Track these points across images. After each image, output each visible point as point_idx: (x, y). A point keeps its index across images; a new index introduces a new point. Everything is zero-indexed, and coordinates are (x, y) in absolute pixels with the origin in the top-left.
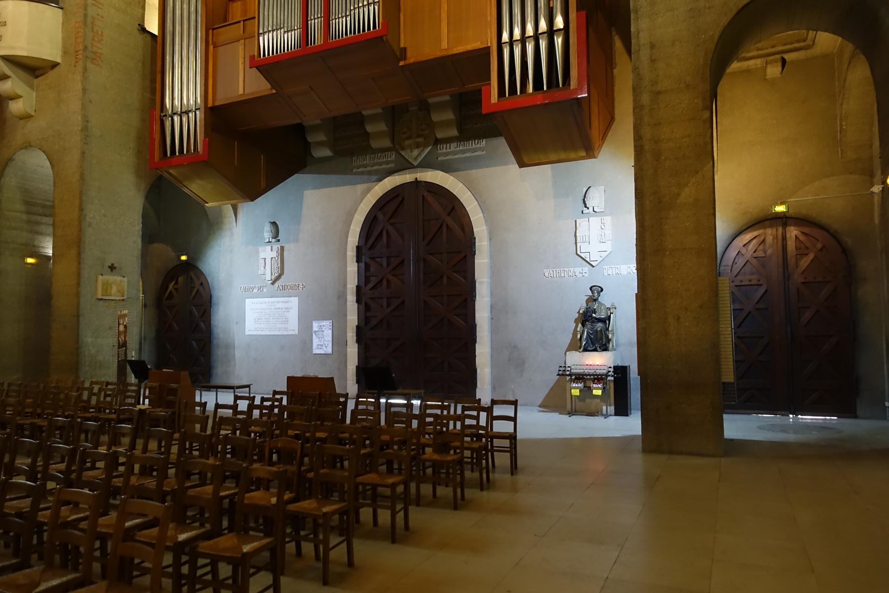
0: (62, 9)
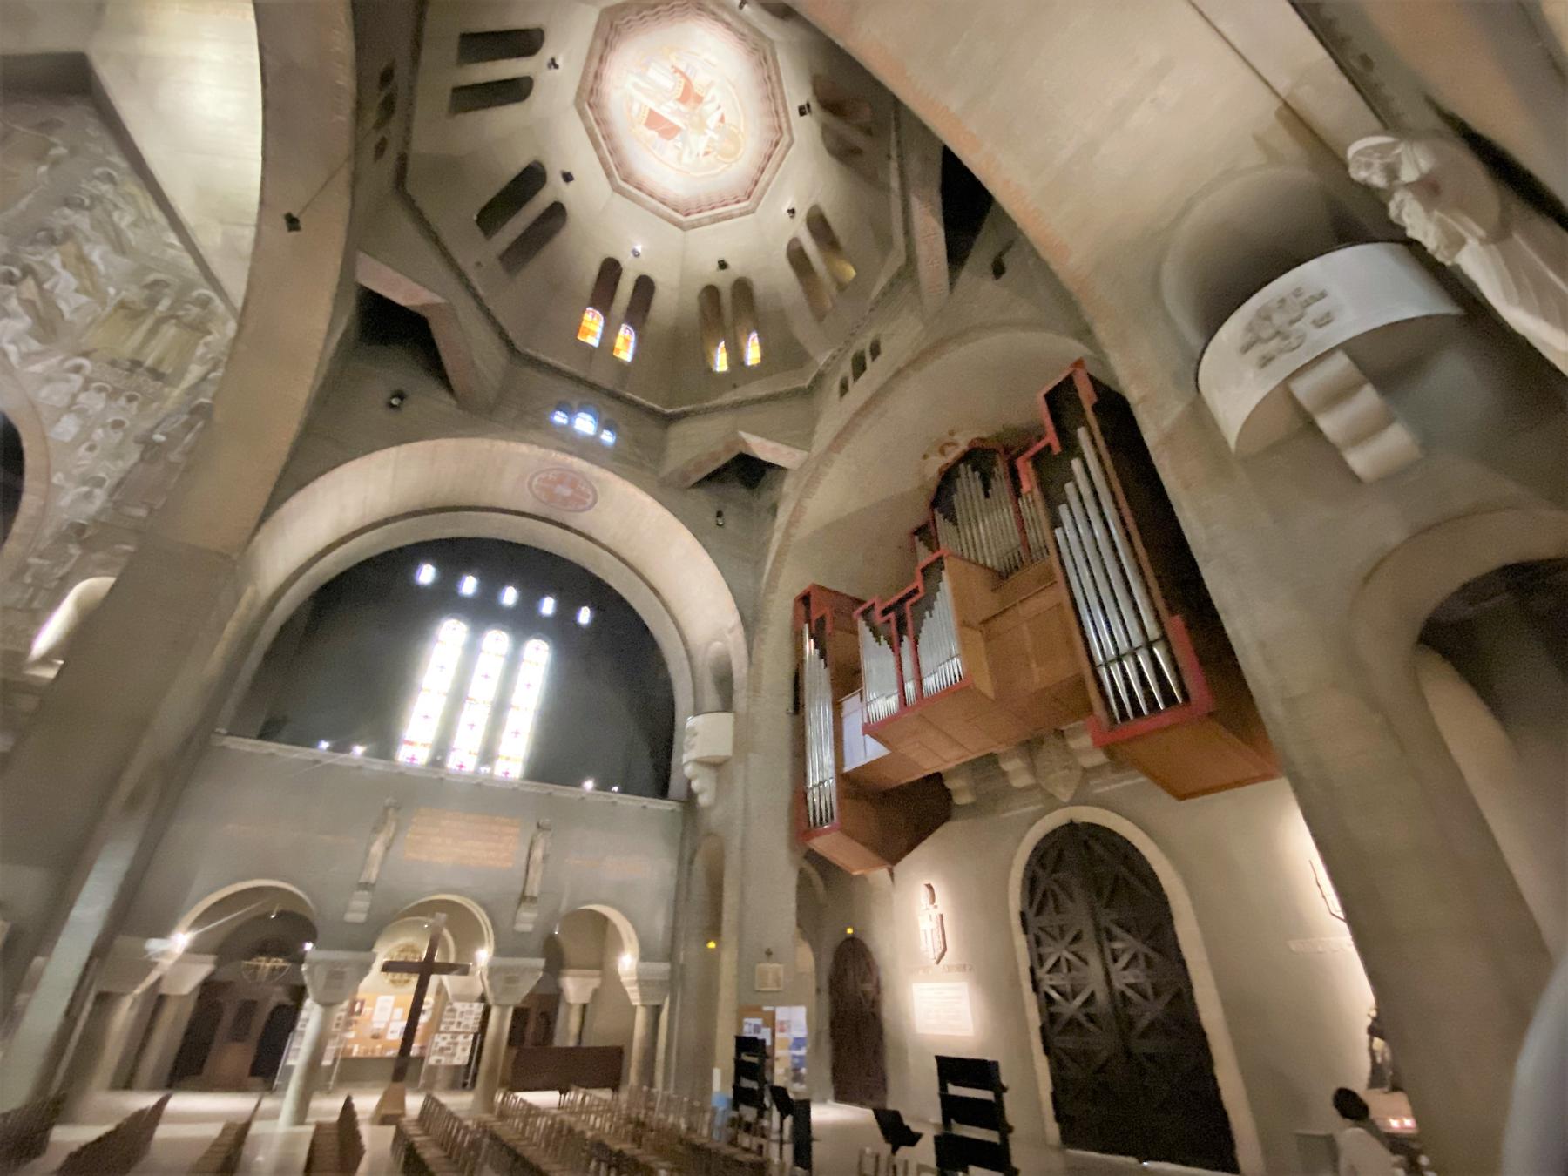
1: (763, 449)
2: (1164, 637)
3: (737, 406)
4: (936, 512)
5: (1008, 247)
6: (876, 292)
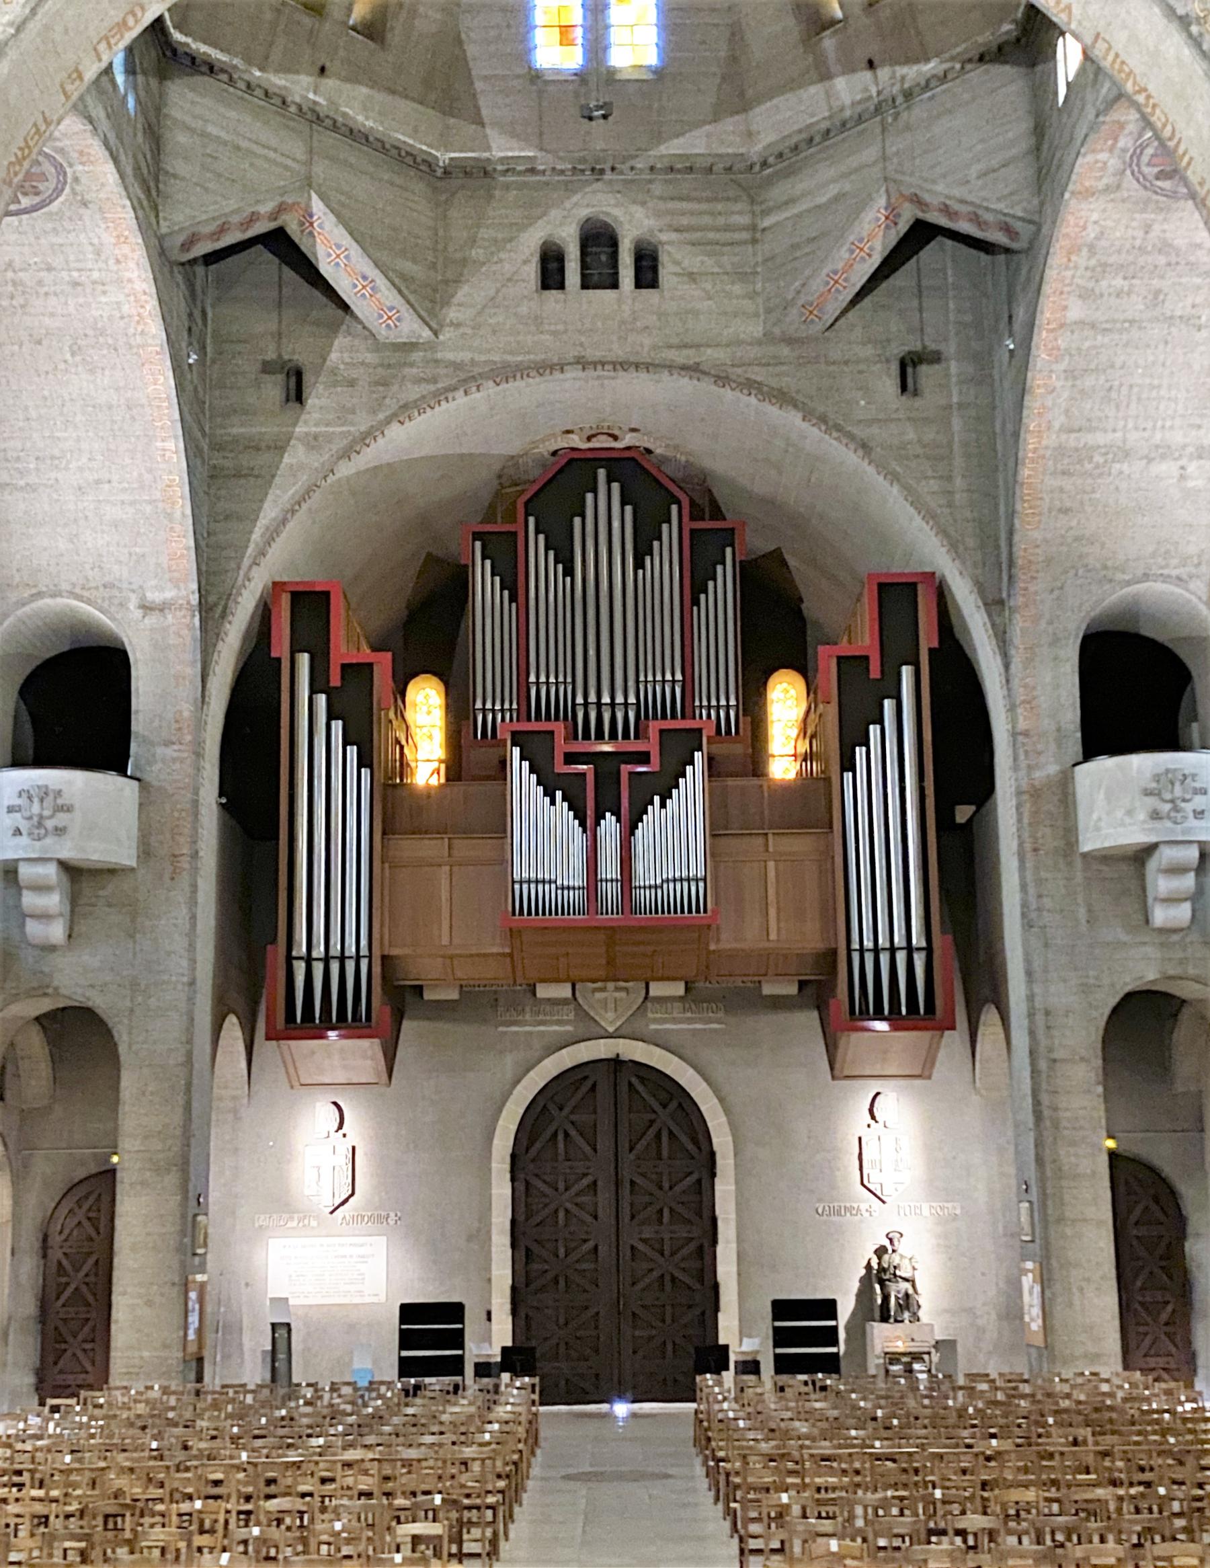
0: (138, 780)
2: (929, 950)
3: (314, 118)
4: (531, 520)
5: (935, 358)
6: (674, 147)
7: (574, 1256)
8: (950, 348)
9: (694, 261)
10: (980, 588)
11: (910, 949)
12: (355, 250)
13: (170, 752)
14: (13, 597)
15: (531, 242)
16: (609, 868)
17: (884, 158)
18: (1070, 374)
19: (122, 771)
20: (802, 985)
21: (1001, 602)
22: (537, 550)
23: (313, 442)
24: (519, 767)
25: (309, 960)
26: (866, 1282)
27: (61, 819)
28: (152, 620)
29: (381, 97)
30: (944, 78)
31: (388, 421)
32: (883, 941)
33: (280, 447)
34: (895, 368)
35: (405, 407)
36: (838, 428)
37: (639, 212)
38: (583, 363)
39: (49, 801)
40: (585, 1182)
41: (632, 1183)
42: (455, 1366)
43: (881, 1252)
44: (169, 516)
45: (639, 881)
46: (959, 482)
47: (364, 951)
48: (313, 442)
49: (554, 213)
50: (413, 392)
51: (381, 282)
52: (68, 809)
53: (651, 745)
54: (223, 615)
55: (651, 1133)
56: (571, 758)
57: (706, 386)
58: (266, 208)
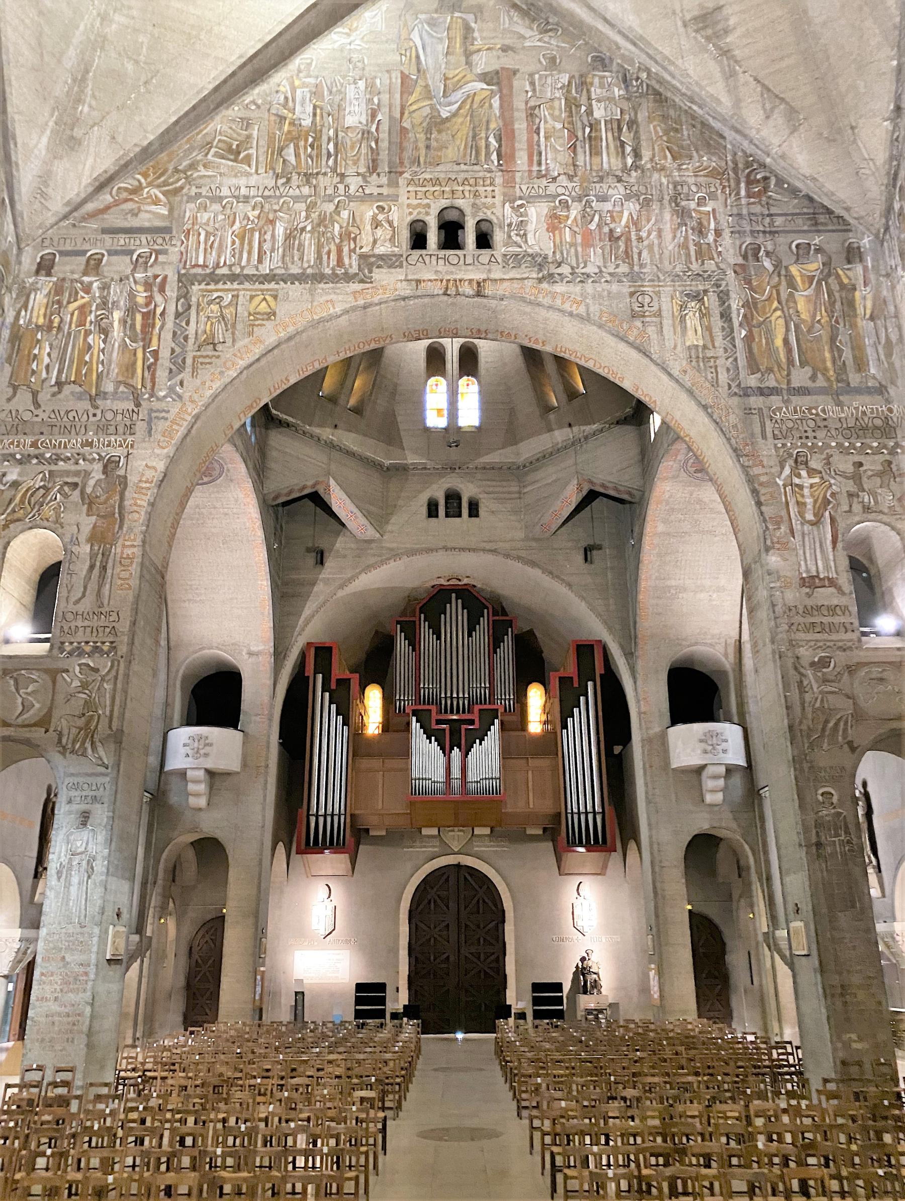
1: (339, 501)
2: (603, 813)
3: (332, 446)
5: (599, 548)
7: (438, 961)
8: (606, 544)
9: (494, 506)
10: (622, 648)
11: (594, 812)
12: (348, 501)
13: (258, 719)
14: (191, 649)
15: (424, 498)
16: (456, 773)
17: (576, 464)
18: (659, 555)
19: (236, 727)
20: (545, 830)
21: (632, 654)
22: (425, 631)
23: (327, 581)
24: (415, 725)
25: (317, 816)
26: (576, 974)
27: (207, 749)
28: (252, 660)
29: (360, 437)
30: (601, 431)
31: (360, 573)
32: (582, 809)
33: (313, 584)
34: (582, 551)
35: (368, 567)
36: (558, 577)
37: (471, 486)
38: (446, 549)
39: (202, 742)
40: (444, 924)
41: (466, 926)
42: (381, 1014)
43: (583, 959)
44: (263, 614)
45: (469, 779)
46: (611, 601)
47: (343, 811)
48: (327, 581)
49: (435, 486)
50: (372, 560)
51: (359, 514)
52: (211, 745)
53: (475, 716)
54: (284, 658)
55: (475, 901)
56: (439, 722)
57: (500, 559)
58: (310, 483)
